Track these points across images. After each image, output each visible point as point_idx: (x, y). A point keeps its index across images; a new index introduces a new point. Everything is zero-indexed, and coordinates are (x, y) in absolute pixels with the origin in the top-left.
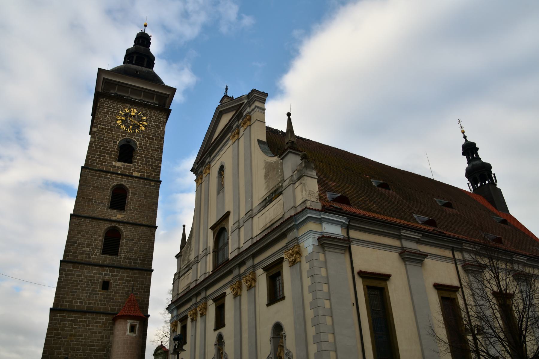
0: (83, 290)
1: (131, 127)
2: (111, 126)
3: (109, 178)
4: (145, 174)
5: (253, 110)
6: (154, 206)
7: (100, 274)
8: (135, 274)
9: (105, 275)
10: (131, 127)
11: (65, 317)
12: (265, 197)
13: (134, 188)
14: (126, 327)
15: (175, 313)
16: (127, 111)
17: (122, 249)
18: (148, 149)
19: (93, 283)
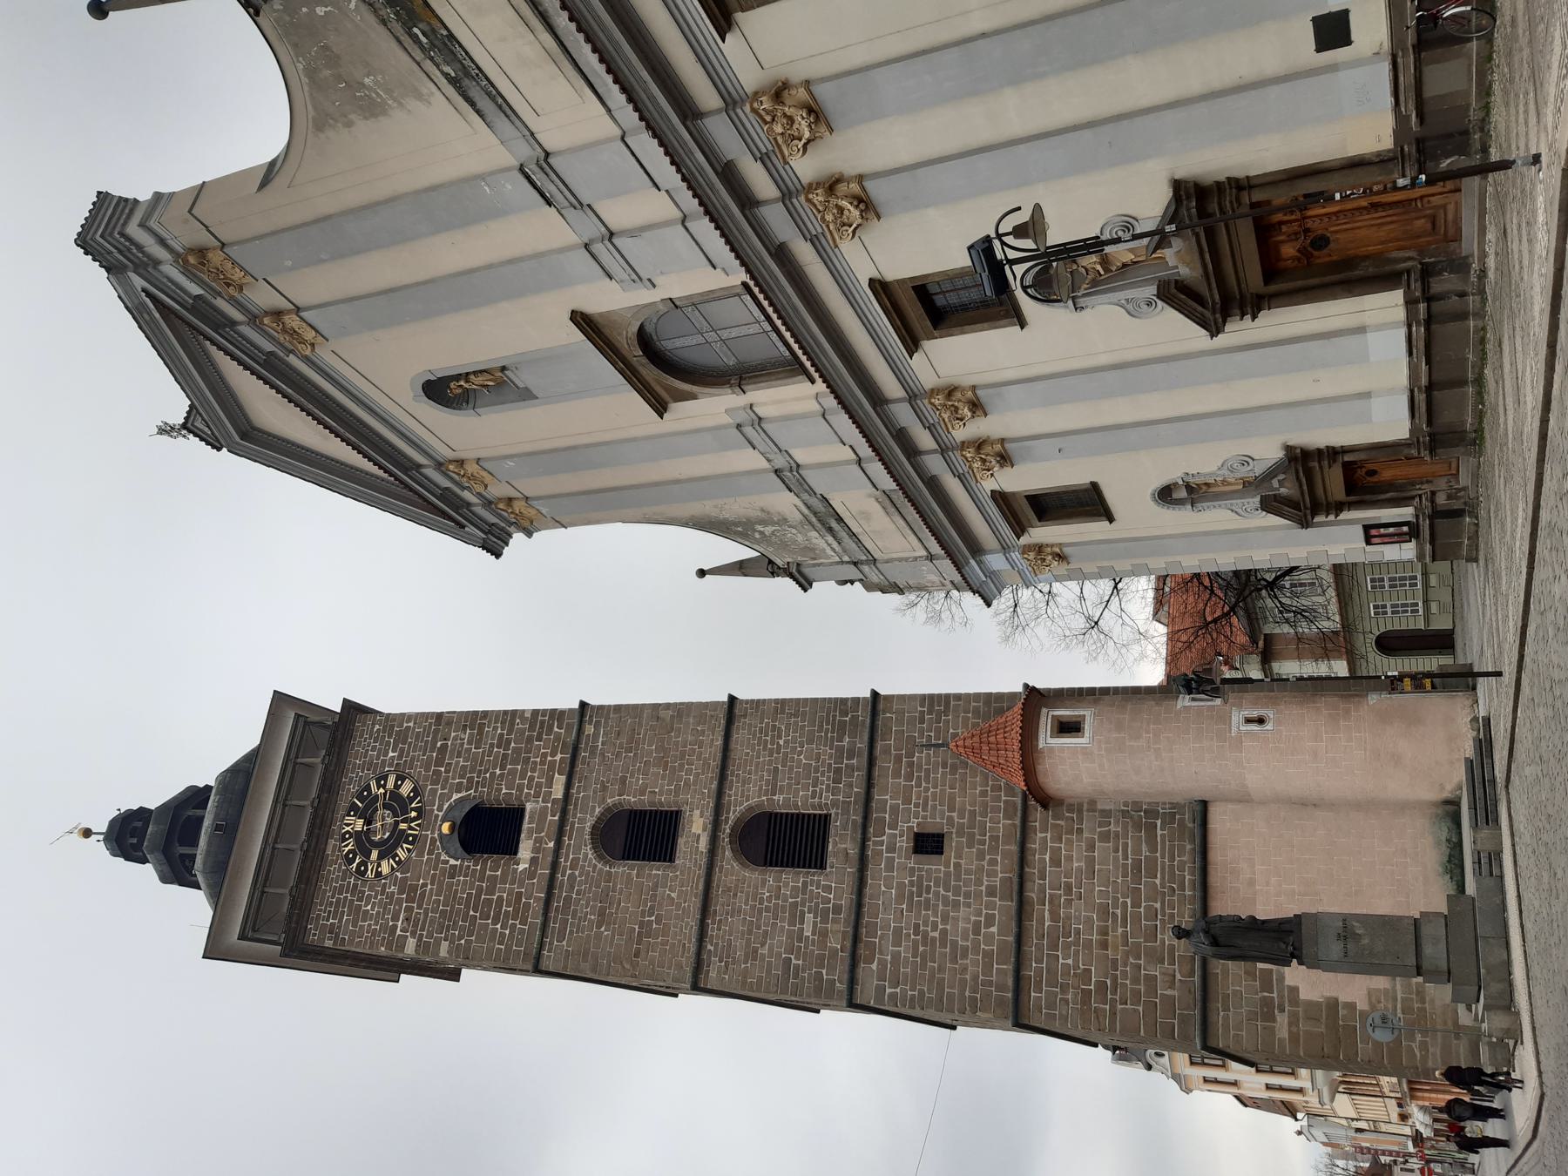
0: (945, 919)
1: (403, 826)
3: (572, 876)
4: (558, 757)
5: (162, 242)
6: (662, 713)
7: (890, 868)
8: (887, 751)
9: (891, 849)
10: (403, 826)
11: (1039, 972)
12: (450, 91)
13: (604, 788)
14: (1062, 749)
15: (996, 561)
16: (350, 845)
17: (805, 804)
18: (474, 760)
19: (920, 886)
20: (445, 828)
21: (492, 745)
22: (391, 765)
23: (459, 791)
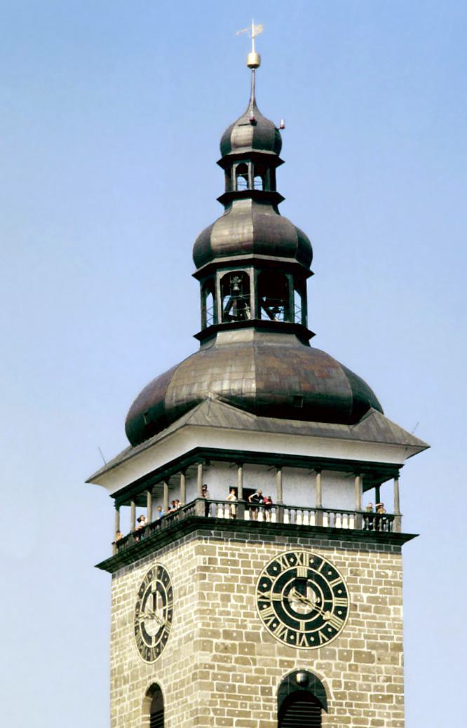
2: (248, 636)
18: (362, 697)
21: (373, 714)
22: (356, 599)
23: (337, 684)
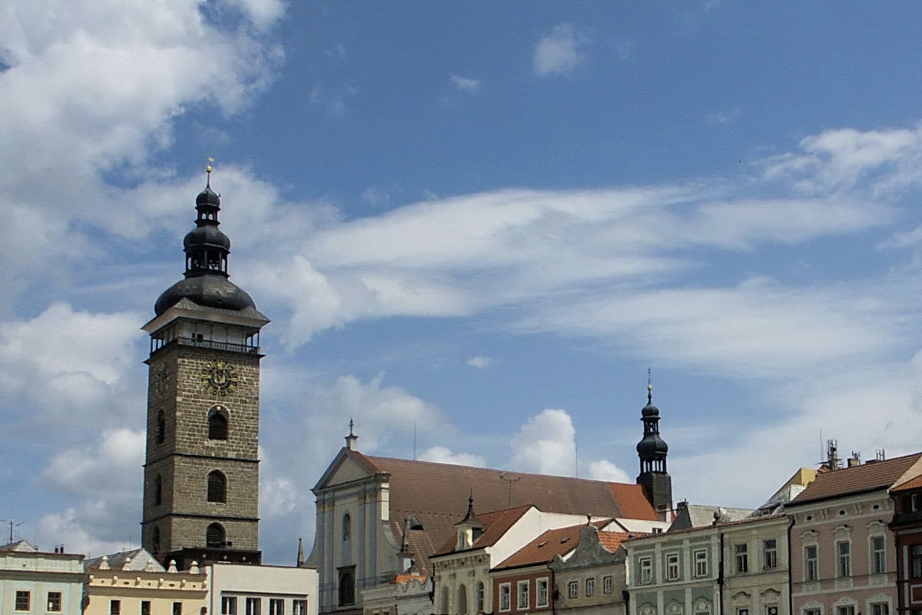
3: (202, 464)
20: (219, 408)
23: (232, 412)
